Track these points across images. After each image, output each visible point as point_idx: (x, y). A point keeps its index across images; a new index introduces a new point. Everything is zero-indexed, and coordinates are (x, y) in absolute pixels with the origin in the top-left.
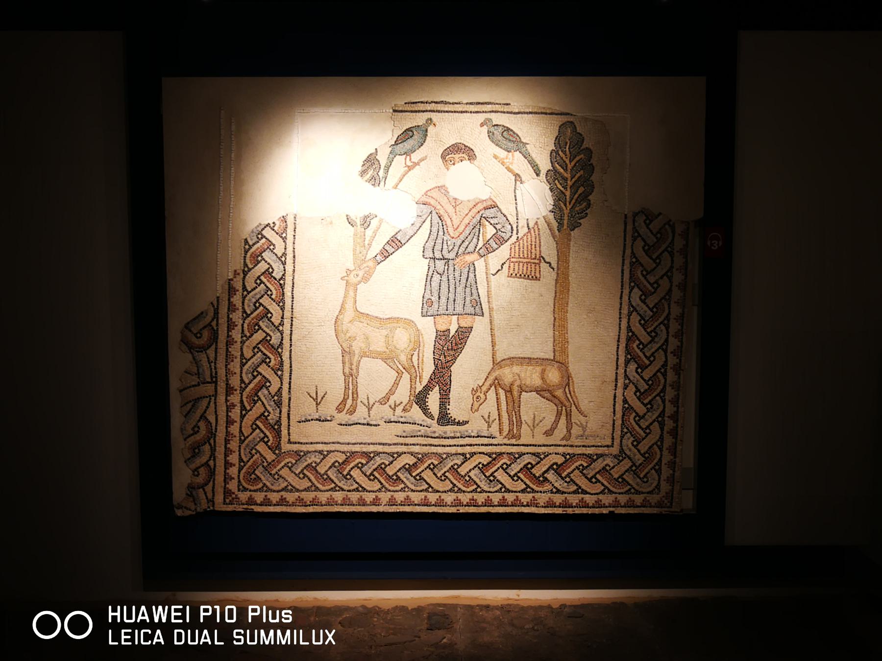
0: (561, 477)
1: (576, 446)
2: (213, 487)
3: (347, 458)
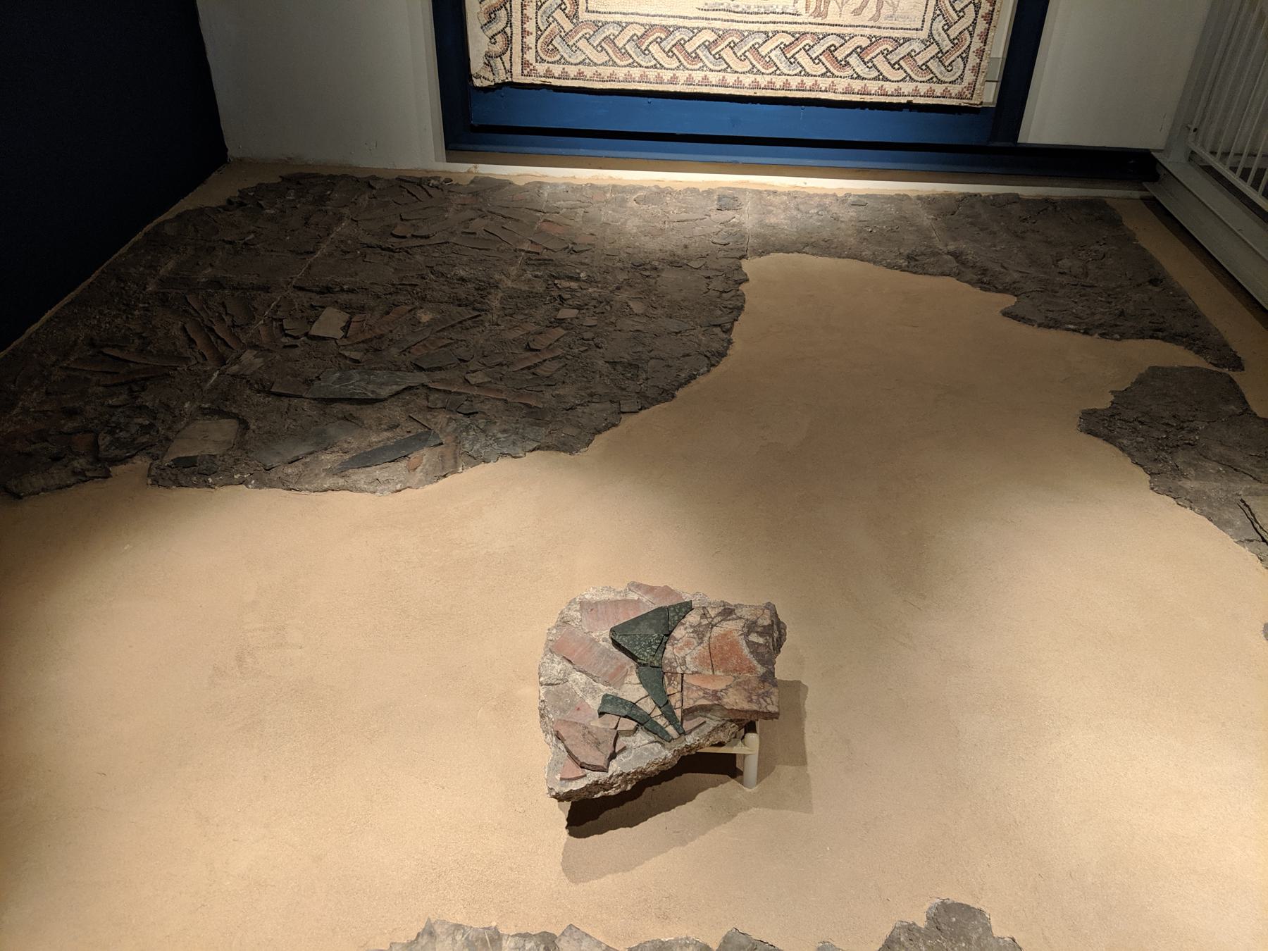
0: (863, 61)
1: (884, 28)
2: (511, 57)
3: (646, 32)
